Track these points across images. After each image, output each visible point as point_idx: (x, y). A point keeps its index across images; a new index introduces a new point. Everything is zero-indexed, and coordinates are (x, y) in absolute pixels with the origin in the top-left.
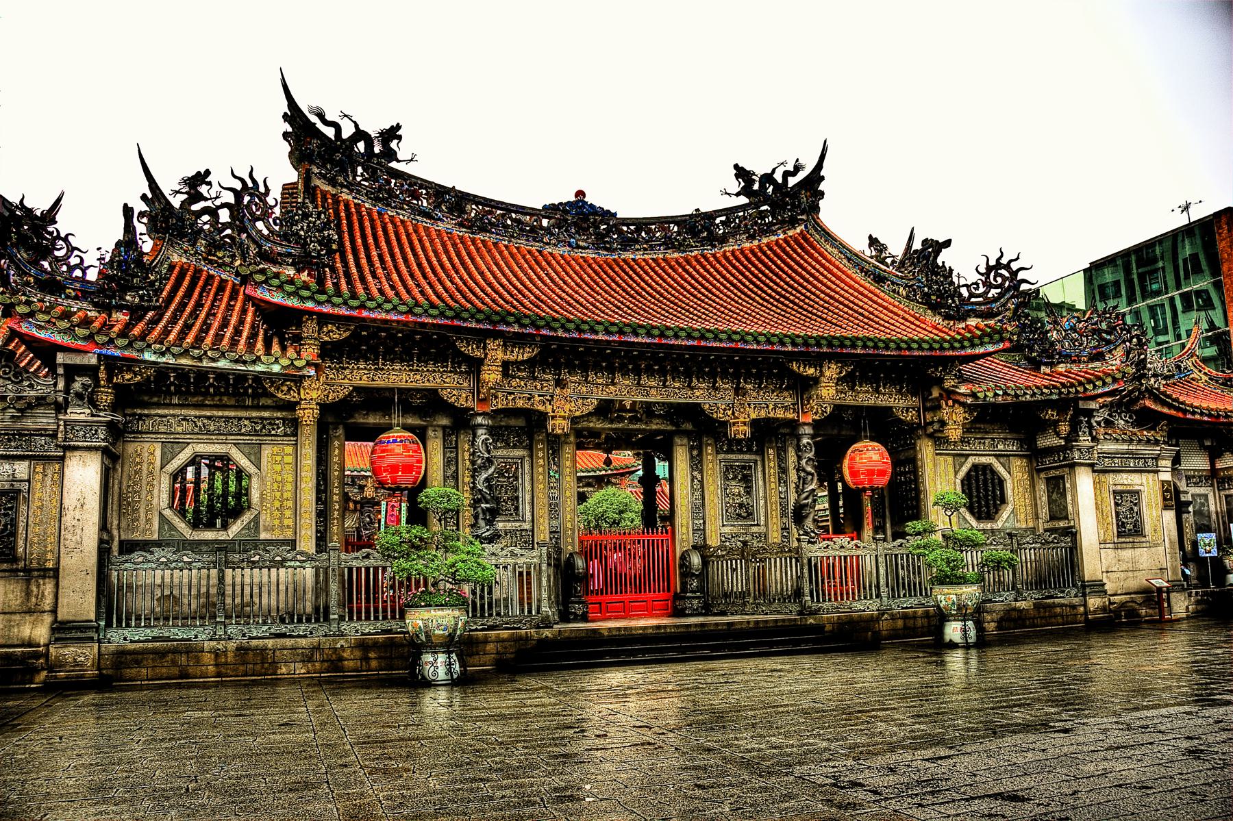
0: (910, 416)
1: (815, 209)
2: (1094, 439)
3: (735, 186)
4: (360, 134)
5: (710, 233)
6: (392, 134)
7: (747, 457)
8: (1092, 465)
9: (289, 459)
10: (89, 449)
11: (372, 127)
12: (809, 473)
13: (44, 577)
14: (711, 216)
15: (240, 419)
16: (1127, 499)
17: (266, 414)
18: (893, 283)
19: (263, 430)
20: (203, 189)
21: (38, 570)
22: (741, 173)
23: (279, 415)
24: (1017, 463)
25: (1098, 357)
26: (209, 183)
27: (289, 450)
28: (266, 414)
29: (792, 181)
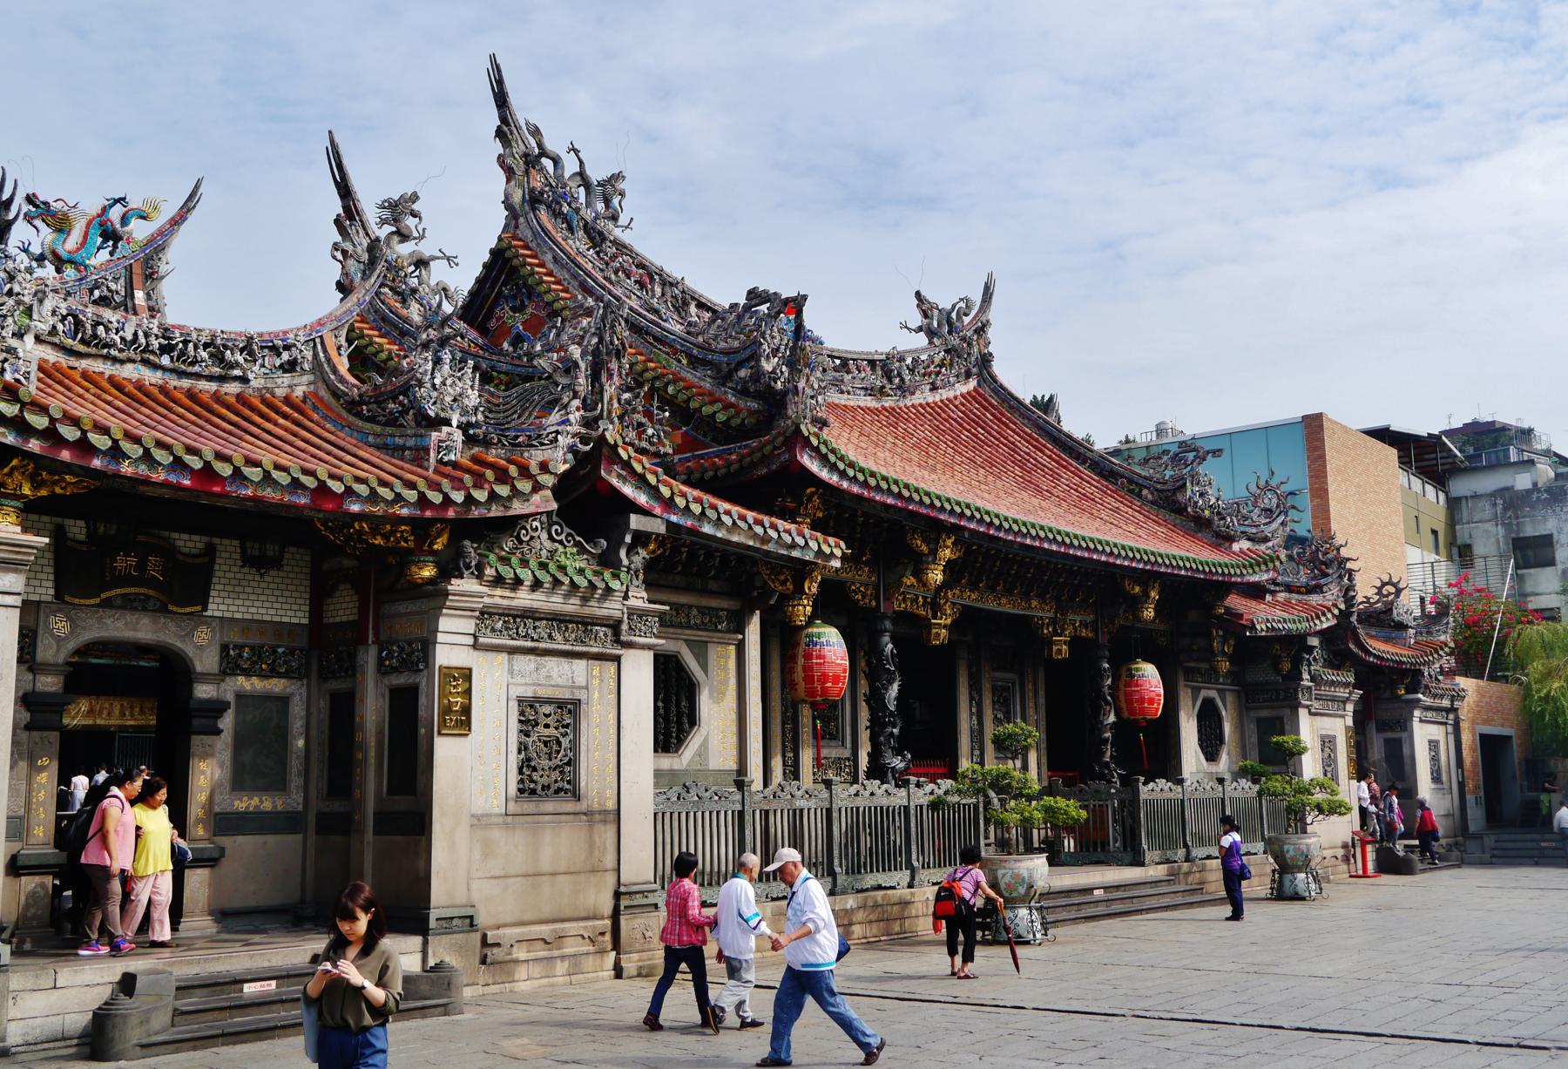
3: (916, 319)
5: (902, 380)
11: (596, 174)
12: (1108, 703)
13: (604, 822)
15: (690, 607)
16: (1327, 742)
17: (714, 603)
18: (1130, 481)
19: (710, 621)
20: (410, 222)
21: (600, 812)
23: (725, 604)
24: (1230, 698)
25: (1317, 589)
27: (732, 649)
28: (714, 603)
29: (967, 320)
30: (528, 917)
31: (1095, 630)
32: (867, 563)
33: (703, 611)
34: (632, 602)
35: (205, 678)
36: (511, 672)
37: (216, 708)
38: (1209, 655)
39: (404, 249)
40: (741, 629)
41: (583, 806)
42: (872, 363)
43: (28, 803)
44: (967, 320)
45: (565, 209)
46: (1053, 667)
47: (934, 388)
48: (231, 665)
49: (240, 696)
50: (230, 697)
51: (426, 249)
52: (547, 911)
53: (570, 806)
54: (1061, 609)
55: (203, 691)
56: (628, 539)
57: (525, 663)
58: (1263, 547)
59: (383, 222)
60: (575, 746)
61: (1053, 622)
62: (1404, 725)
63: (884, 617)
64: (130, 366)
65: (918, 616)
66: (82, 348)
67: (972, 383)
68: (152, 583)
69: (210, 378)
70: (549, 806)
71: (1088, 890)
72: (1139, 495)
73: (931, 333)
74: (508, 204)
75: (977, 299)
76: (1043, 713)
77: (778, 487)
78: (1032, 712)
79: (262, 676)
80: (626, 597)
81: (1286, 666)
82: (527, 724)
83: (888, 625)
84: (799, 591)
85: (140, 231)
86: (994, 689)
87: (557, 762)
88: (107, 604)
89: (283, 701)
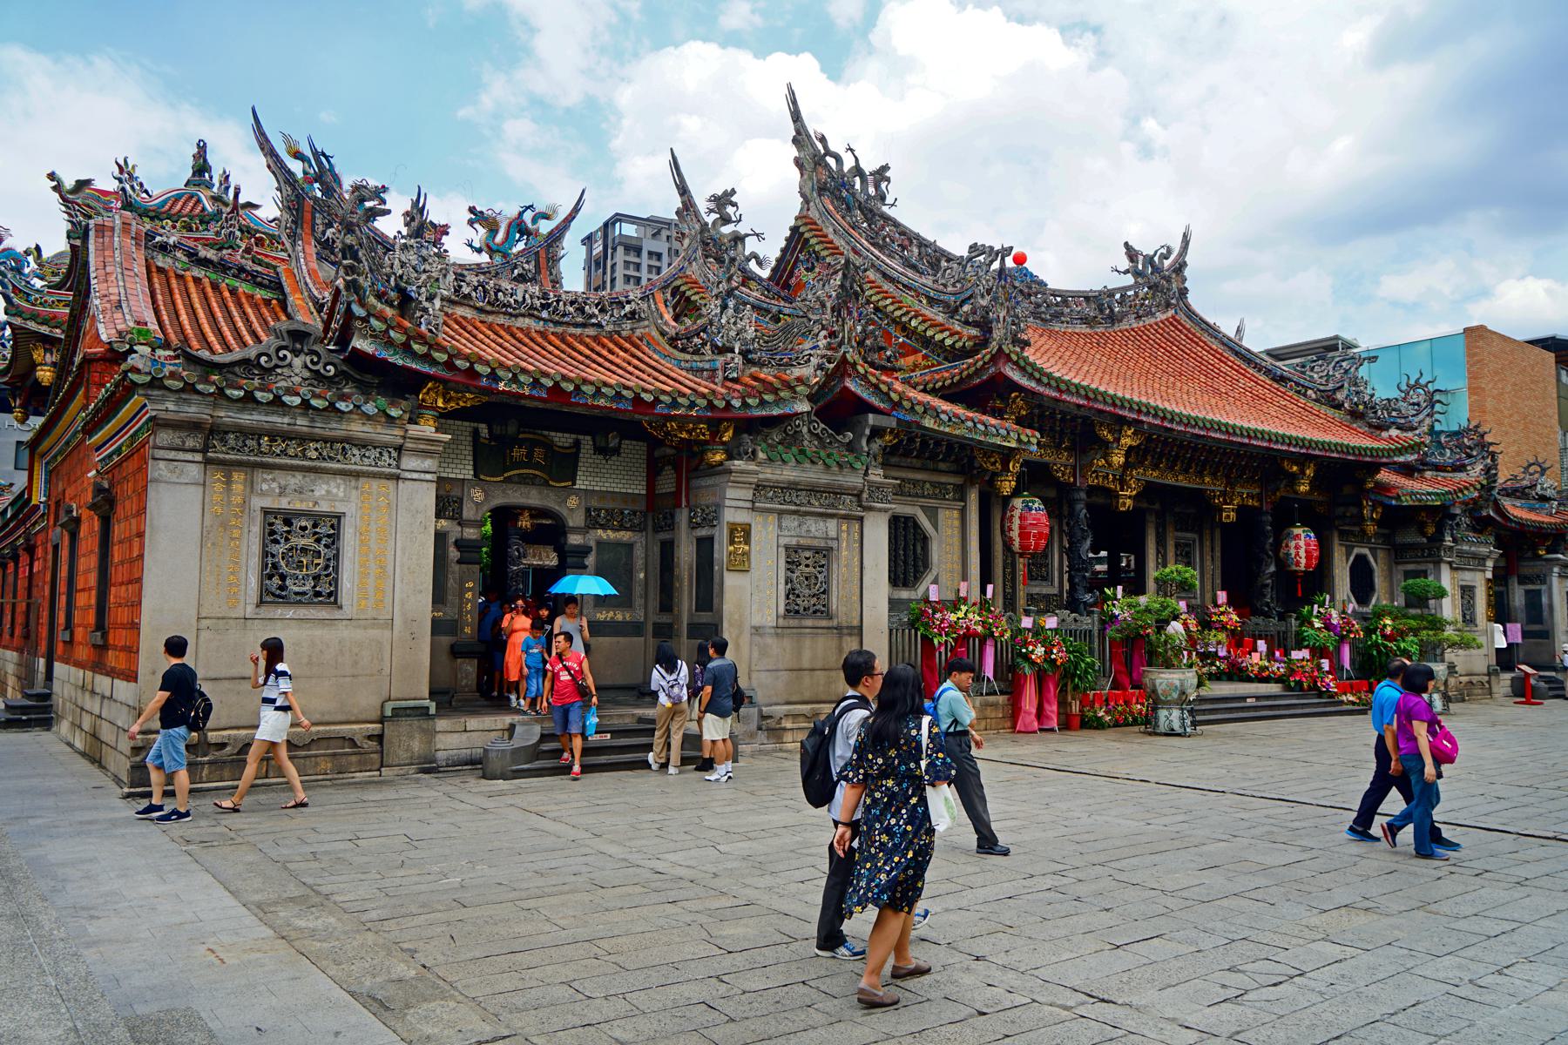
0: (1321, 510)
1: (1183, 292)
2: (1455, 540)
3: (1125, 264)
4: (858, 170)
5: (1112, 311)
6: (881, 174)
7: (1189, 535)
8: (1450, 563)
9: (957, 523)
10: (880, 510)
11: (868, 166)
14: (1111, 294)
16: (1467, 591)
17: (943, 479)
19: (940, 491)
20: (730, 210)
22: (1132, 254)
23: (952, 480)
24: (1381, 554)
25: (1460, 468)
26: (734, 205)
27: (956, 514)
28: (943, 479)
29: (1167, 263)
30: (794, 699)
31: (1260, 500)
32: (1066, 449)
33: (934, 485)
34: (872, 478)
35: (576, 530)
36: (780, 527)
37: (584, 551)
38: (1360, 519)
39: (727, 229)
40: (963, 499)
41: (835, 623)
42: (1087, 299)
43: (460, 612)
44: (1167, 263)
45: (844, 194)
46: (1226, 527)
47: (1139, 317)
48: (592, 522)
49: (599, 543)
50: (592, 544)
51: (742, 229)
52: (807, 696)
53: (824, 623)
54: (1230, 483)
55: (574, 540)
56: (867, 432)
57: (791, 522)
58: (1410, 434)
59: (711, 211)
60: (827, 581)
61: (1224, 494)
62: (1543, 579)
63: (1079, 489)
64: (521, 319)
65: (1109, 490)
66: (489, 308)
67: (1171, 312)
68: (537, 466)
69: (576, 325)
70: (809, 623)
71: (1244, 699)
72: (1305, 395)
73: (1137, 274)
74: (803, 195)
75: (1176, 247)
76: (1218, 563)
77: (985, 393)
78: (1209, 563)
79: (614, 530)
80: (866, 474)
81: (1431, 530)
82: (792, 564)
83: (1083, 495)
84: (1006, 469)
85: (545, 227)
86: (1177, 546)
87: (814, 591)
88: (508, 480)
89: (630, 546)
